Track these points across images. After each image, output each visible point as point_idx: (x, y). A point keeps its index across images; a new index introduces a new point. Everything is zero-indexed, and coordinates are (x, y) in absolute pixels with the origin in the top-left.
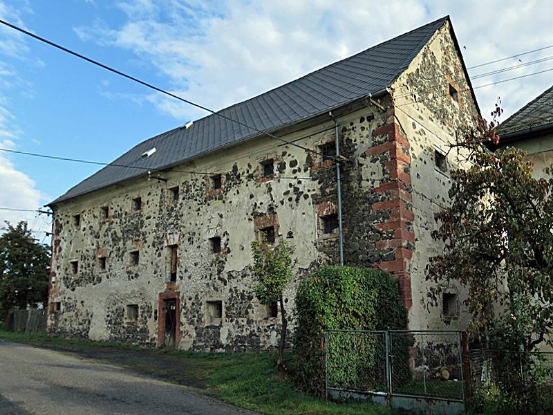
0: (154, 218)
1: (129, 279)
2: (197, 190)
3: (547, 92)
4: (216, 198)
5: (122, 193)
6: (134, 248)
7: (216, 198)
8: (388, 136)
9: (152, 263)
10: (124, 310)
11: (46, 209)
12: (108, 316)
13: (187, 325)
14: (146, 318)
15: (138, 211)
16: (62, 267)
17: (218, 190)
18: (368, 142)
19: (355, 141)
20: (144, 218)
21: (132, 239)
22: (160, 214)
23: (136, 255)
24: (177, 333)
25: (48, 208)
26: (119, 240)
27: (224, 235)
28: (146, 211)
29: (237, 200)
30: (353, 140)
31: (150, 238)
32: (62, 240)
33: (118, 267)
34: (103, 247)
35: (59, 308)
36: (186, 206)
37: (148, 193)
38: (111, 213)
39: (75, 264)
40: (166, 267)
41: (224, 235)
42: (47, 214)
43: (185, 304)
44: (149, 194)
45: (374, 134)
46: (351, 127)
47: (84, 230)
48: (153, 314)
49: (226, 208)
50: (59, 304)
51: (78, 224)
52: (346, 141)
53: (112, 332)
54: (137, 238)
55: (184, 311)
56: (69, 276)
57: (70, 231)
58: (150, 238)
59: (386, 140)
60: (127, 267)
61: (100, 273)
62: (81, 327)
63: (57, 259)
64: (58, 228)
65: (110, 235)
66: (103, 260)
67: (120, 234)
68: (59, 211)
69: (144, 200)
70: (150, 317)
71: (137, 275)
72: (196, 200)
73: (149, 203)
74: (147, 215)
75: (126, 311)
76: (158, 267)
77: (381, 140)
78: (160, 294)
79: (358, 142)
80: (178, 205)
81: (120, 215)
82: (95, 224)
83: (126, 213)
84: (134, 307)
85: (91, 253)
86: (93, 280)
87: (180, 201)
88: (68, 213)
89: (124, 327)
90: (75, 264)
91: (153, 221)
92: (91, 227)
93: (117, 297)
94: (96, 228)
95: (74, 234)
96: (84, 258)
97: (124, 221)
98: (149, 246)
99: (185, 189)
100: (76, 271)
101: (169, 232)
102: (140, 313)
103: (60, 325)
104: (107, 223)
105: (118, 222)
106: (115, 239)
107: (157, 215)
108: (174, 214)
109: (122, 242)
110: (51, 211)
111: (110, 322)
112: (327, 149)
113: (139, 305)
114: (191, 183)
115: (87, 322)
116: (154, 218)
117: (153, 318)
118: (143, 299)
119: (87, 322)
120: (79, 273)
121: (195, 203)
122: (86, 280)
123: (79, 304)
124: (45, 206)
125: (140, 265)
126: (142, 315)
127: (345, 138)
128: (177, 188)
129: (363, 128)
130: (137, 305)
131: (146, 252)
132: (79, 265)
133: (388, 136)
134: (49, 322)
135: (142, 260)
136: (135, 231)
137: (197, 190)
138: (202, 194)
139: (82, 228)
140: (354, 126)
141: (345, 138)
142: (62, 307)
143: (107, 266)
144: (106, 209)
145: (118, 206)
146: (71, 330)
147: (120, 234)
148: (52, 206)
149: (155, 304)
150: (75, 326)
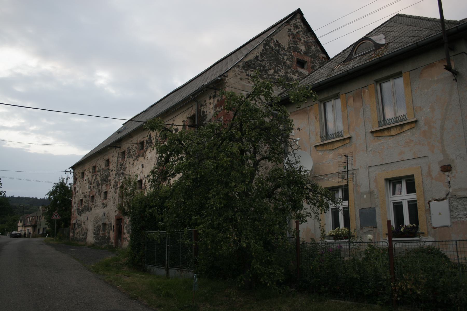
0: (115, 170)
1: (103, 207)
2: (133, 152)
3: (382, 24)
4: (141, 155)
5: (102, 157)
6: (106, 189)
7: (141, 155)
8: (222, 107)
9: (113, 198)
10: (101, 226)
11: (69, 170)
12: (94, 230)
13: (126, 234)
14: (109, 230)
15: (108, 167)
16: (76, 203)
17: (142, 151)
18: (212, 112)
19: (206, 112)
20: (110, 171)
21: (105, 184)
22: (117, 168)
23: (106, 193)
24: (122, 239)
25: (71, 169)
26: (99, 185)
27: (144, 178)
28: (111, 167)
29: (150, 156)
30: (205, 111)
31: (112, 183)
32: (77, 187)
33: (99, 200)
34: (93, 189)
35: (75, 227)
36: (129, 161)
37: (112, 156)
38: (97, 169)
39: (82, 200)
40: (119, 200)
41: (144, 178)
42: (70, 173)
43: (126, 222)
44: (113, 156)
45: (216, 106)
46: (204, 104)
47: (85, 181)
48: (112, 228)
49: (145, 161)
50: (75, 224)
51: (83, 177)
52: (202, 112)
53: (95, 240)
54: (107, 183)
55: (125, 225)
56: (79, 208)
57: (80, 182)
58: (112, 183)
59: (222, 109)
60: (103, 201)
61: (91, 205)
62: (83, 237)
63: (75, 198)
64: (75, 179)
65: (96, 182)
66: (93, 197)
67: (100, 182)
68: (76, 170)
69: (110, 161)
70: (111, 230)
71: (106, 206)
72: (132, 158)
73: (113, 162)
74: (111, 169)
75: (101, 227)
76: (115, 200)
77: (219, 110)
78: (116, 216)
79: (208, 113)
80: (125, 162)
81: (100, 170)
82: (90, 176)
83: (103, 169)
84: (104, 224)
85: (88, 194)
86: (89, 209)
87: (126, 159)
88: (79, 170)
89: (100, 237)
90: (82, 200)
91: (114, 172)
92: (88, 178)
93: (98, 218)
94: (90, 179)
95: (82, 183)
96: (85, 196)
97: (102, 173)
98: (112, 188)
99: (128, 152)
100: (82, 204)
101: (120, 178)
102: (107, 228)
103: (75, 236)
104: (95, 176)
105: (99, 174)
106: (98, 185)
107: (115, 169)
108: (123, 167)
109: (101, 186)
110: (72, 171)
111: (95, 234)
112: (192, 118)
113: (107, 223)
114: (131, 147)
115: (86, 234)
116: (115, 170)
117: (112, 230)
118: (108, 219)
119: (86, 234)
120: (83, 205)
121: (132, 160)
122: (86, 209)
123: (83, 224)
124: (69, 168)
125: (108, 199)
126: (108, 229)
127: (202, 111)
128: (125, 151)
129: (210, 103)
130: (106, 223)
131: (110, 191)
132: (83, 201)
133: (222, 107)
134: (71, 234)
135: (109, 195)
136: (106, 179)
137: (133, 152)
138: (135, 154)
139: (85, 180)
140: (206, 103)
141: (202, 111)
142: (76, 226)
143: (94, 201)
144: (94, 167)
145: (100, 165)
146: (80, 239)
147: (100, 182)
148: (73, 167)
149: (113, 223)
150: (81, 236)
